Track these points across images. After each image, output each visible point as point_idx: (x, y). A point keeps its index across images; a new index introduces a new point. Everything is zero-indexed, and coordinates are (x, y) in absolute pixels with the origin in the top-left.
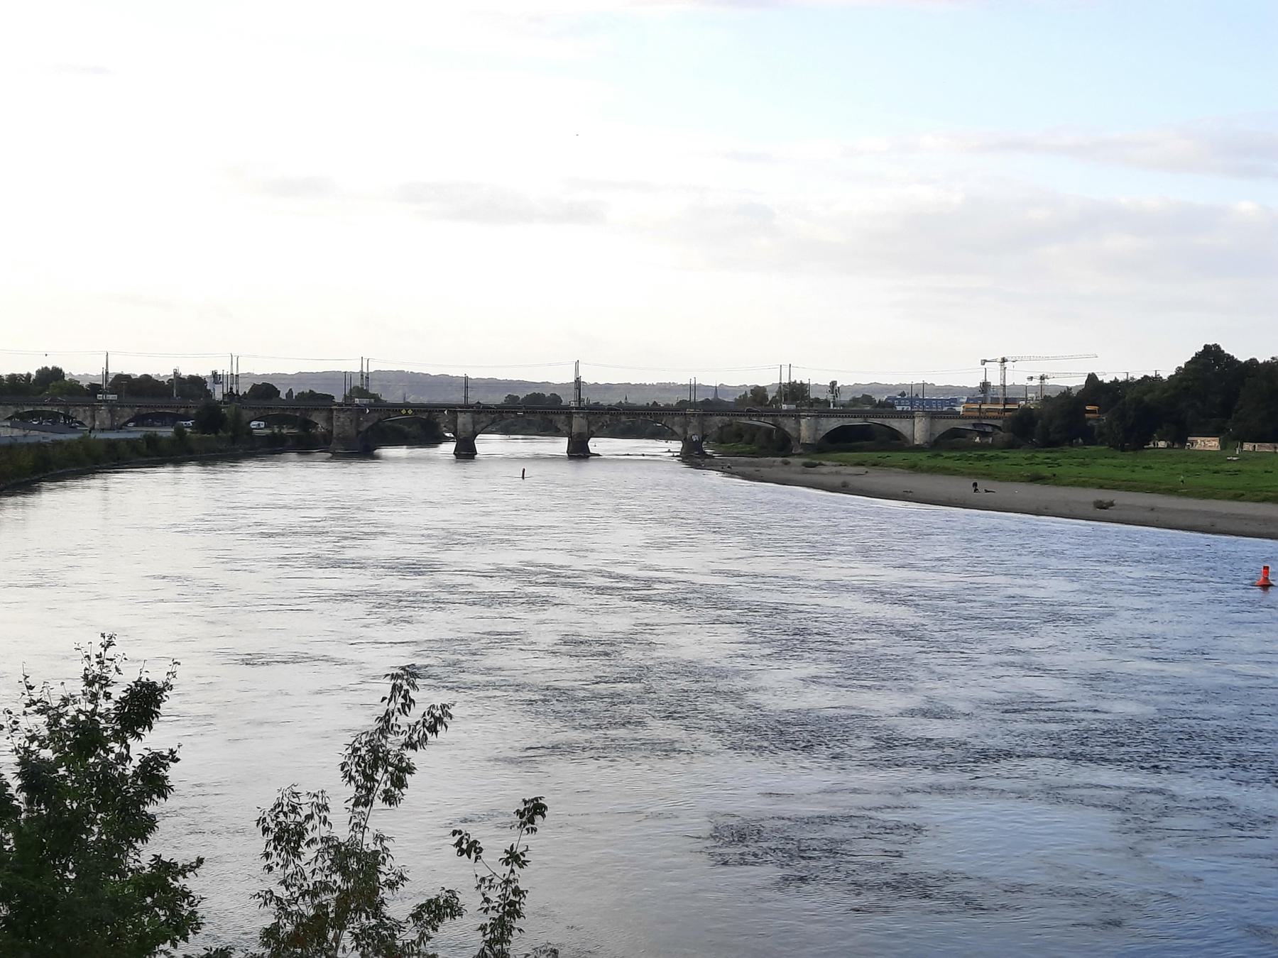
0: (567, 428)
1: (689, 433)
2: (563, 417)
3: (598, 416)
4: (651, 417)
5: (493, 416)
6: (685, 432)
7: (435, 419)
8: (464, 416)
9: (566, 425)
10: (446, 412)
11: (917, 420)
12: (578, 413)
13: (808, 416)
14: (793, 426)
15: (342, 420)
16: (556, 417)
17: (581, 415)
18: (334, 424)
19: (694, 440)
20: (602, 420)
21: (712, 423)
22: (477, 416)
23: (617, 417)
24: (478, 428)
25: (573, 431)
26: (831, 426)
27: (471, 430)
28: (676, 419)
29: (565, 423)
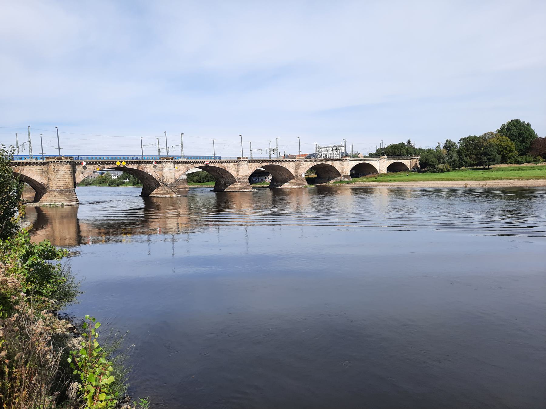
0: (235, 172)
1: (299, 172)
2: (232, 164)
5: (187, 165)
7: (144, 170)
8: (170, 165)
10: (154, 163)
14: (339, 166)
15: (61, 172)
18: (52, 177)
21: (306, 166)
25: (239, 174)
26: (352, 165)
28: (291, 163)
29: (234, 169)
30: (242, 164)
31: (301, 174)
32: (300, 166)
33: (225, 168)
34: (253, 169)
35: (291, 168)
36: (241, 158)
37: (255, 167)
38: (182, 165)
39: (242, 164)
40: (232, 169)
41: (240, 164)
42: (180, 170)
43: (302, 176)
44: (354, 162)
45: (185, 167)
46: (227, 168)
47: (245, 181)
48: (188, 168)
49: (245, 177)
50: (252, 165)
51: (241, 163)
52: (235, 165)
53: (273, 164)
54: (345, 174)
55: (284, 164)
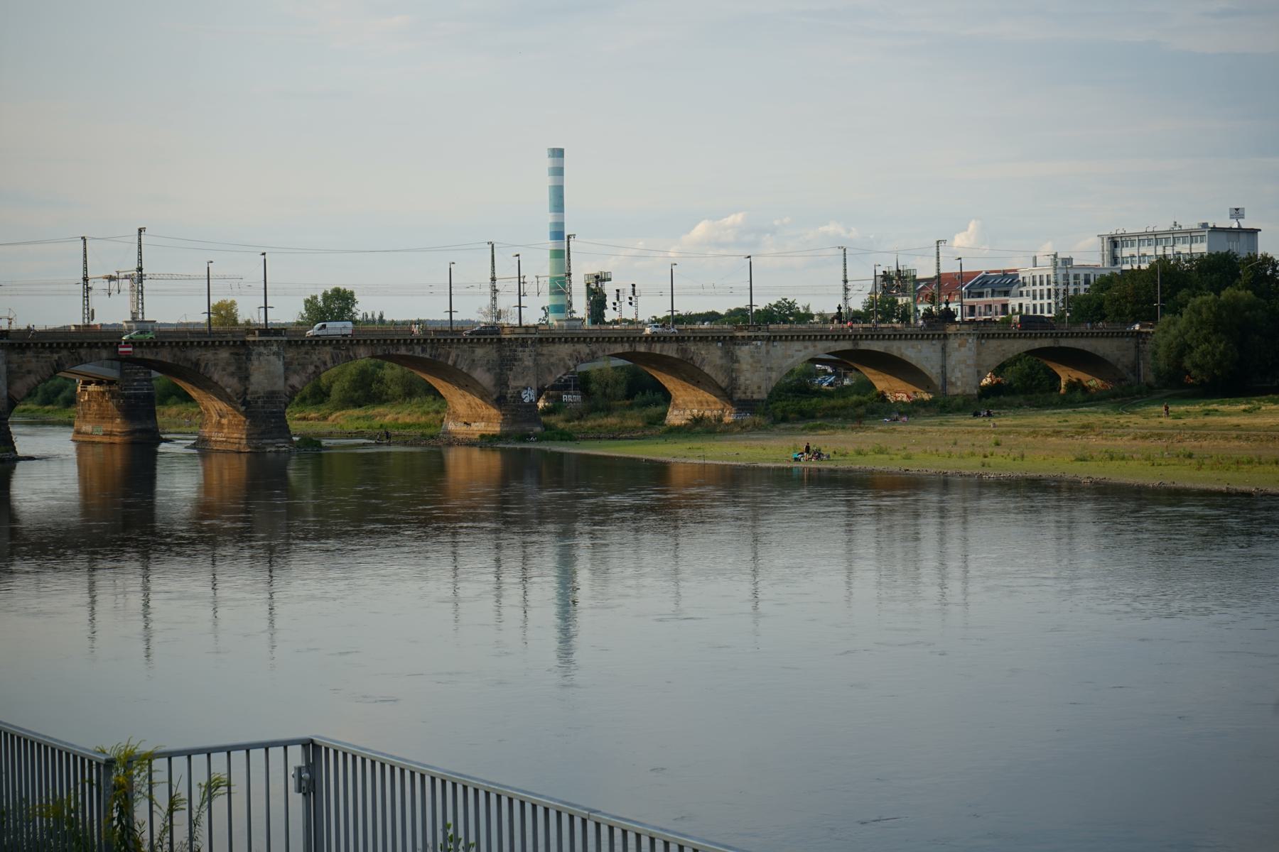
0: (236, 380)
1: (512, 383)
2: (224, 354)
3: (303, 349)
4: (424, 350)
5: (56, 356)
6: (502, 382)
9: (232, 374)
11: (953, 343)
12: (266, 344)
13: (756, 338)
14: (719, 362)
16: (209, 355)
17: (275, 348)
19: (527, 400)
20: (315, 357)
21: (552, 360)
22: (15, 357)
23: (348, 349)
24: (20, 387)
25: (252, 388)
27: (5, 393)
28: (480, 352)
29: (232, 369)
30: (260, 354)
31: (519, 393)
32: (515, 360)
33: (197, 364)
34: (311, 369)
35: (479, 369)
36: (254, 333)
37: (318, 364)
38: (38, 357)
39: (260, 354)
40: (224, 369)
41: (254, 353)
42: (29, 372)
43: (521, 397)
44: (797, 345)
45: (46, 362)
46: (203, 365)
47: (265, 412)
48: (58, 365)
49: (267, 397)
50: (307, 356)
51: (257, 350)
52: (237, 354)
53: (398, 353)
54: (745, 393)
55: (449, 353)
